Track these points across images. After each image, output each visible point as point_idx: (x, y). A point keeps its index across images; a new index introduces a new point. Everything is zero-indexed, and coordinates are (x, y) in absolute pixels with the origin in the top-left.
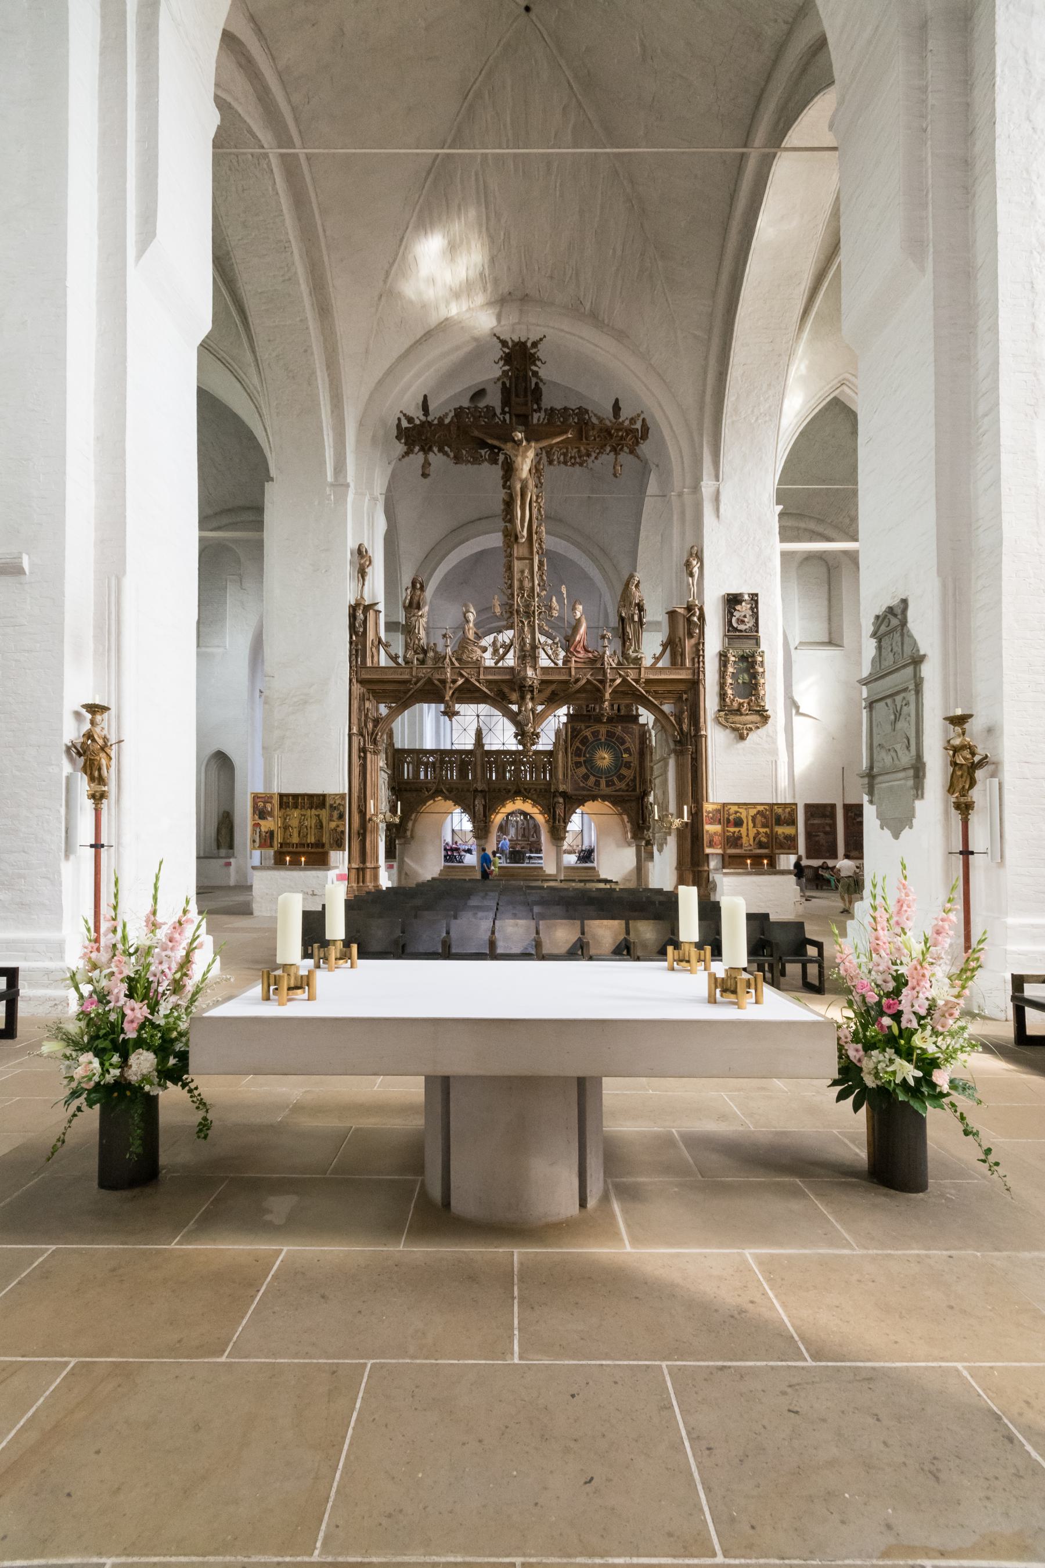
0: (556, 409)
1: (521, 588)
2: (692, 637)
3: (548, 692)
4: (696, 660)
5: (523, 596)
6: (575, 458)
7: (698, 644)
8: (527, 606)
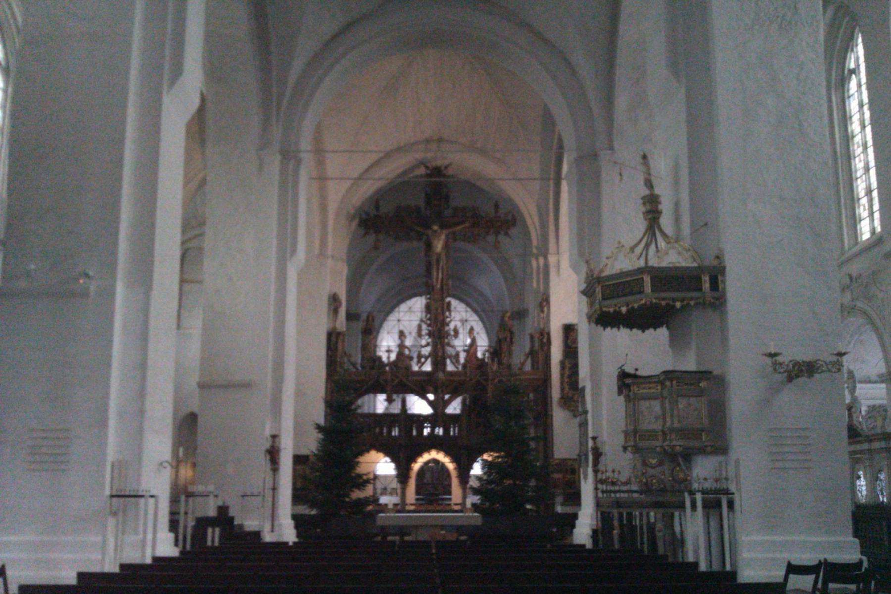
1: (436, 319)
5: (437, 325)
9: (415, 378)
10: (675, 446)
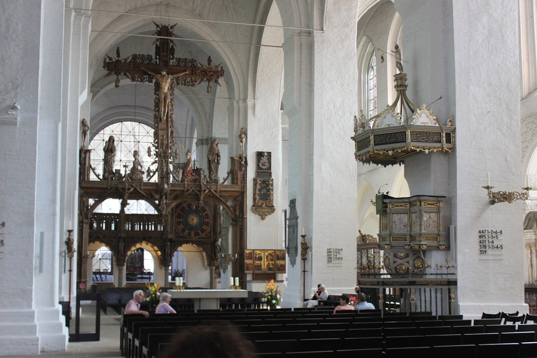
0: (181, 59)
1: (162, 144)
3: (173, 195)
4: (243, 182)
5: (163, 148)
7: (244, 174)
9: (146, 188)
10: (422, 245)
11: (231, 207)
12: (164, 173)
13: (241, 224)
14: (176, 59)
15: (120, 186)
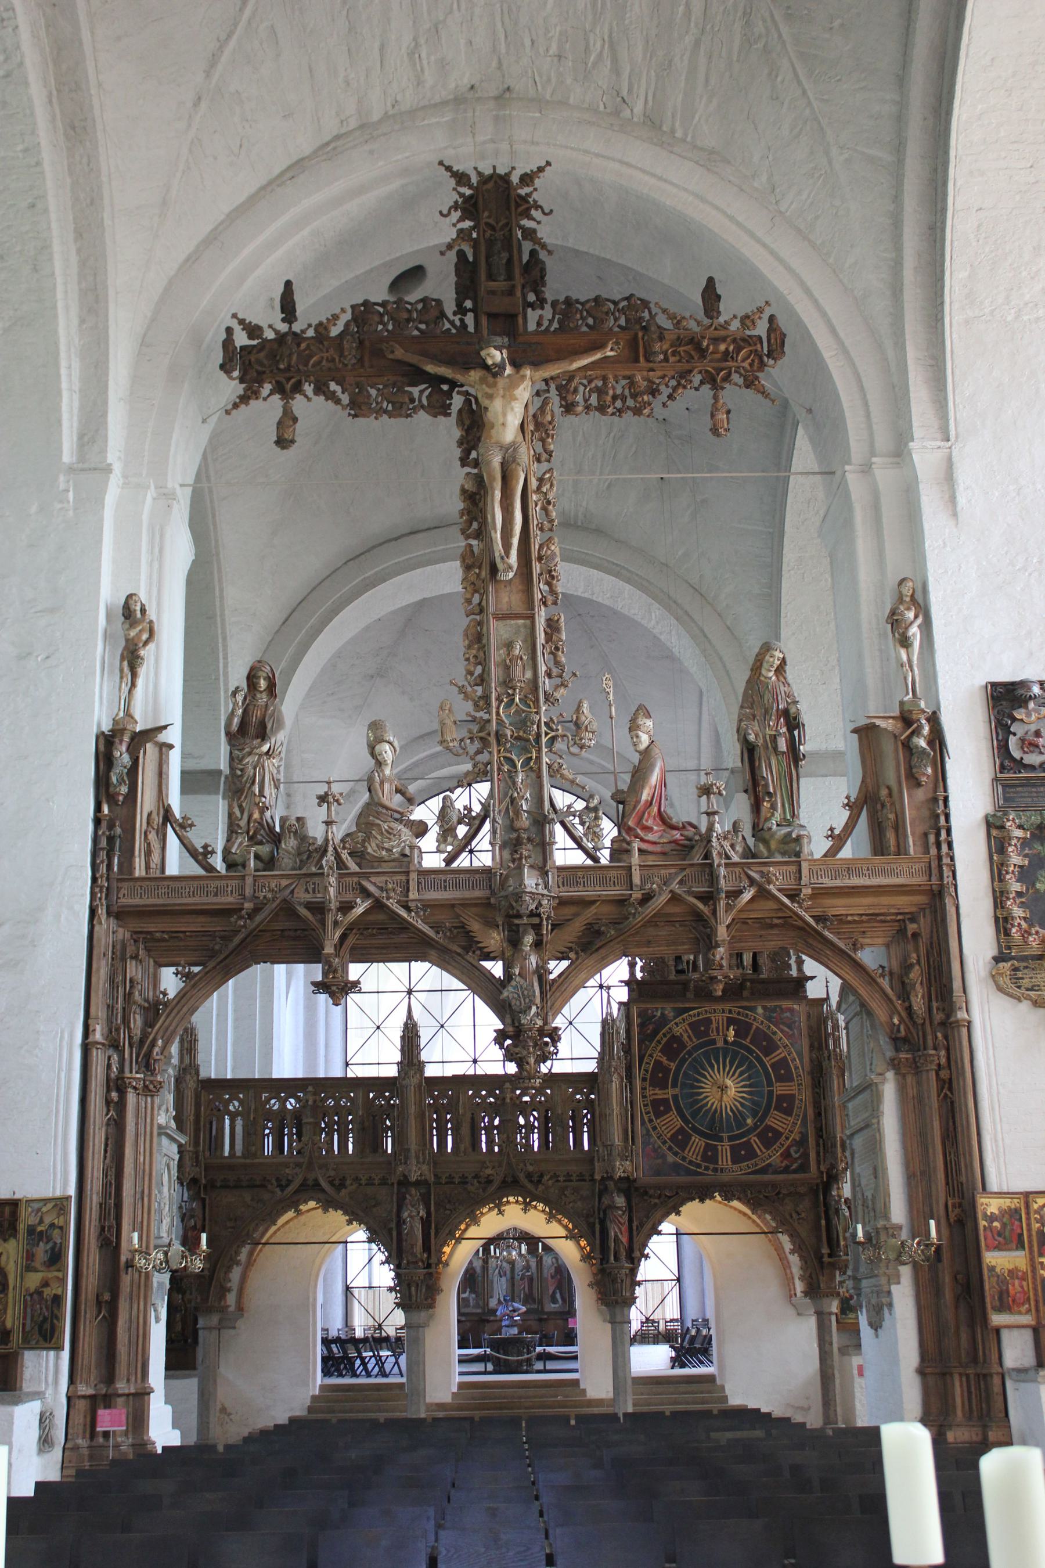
0: (577, 301)
1: (507, 683)
2: (919, 784)
3: (576, 928)
4: (932, 838)
6: (624, 399)
7: (935, 800)
8: (523, 723)
9: (433, 895)
11: (882, 976)
12: (525, 821)
13: (943, 1061)
14: (554, 304)
15: (302, 896)
